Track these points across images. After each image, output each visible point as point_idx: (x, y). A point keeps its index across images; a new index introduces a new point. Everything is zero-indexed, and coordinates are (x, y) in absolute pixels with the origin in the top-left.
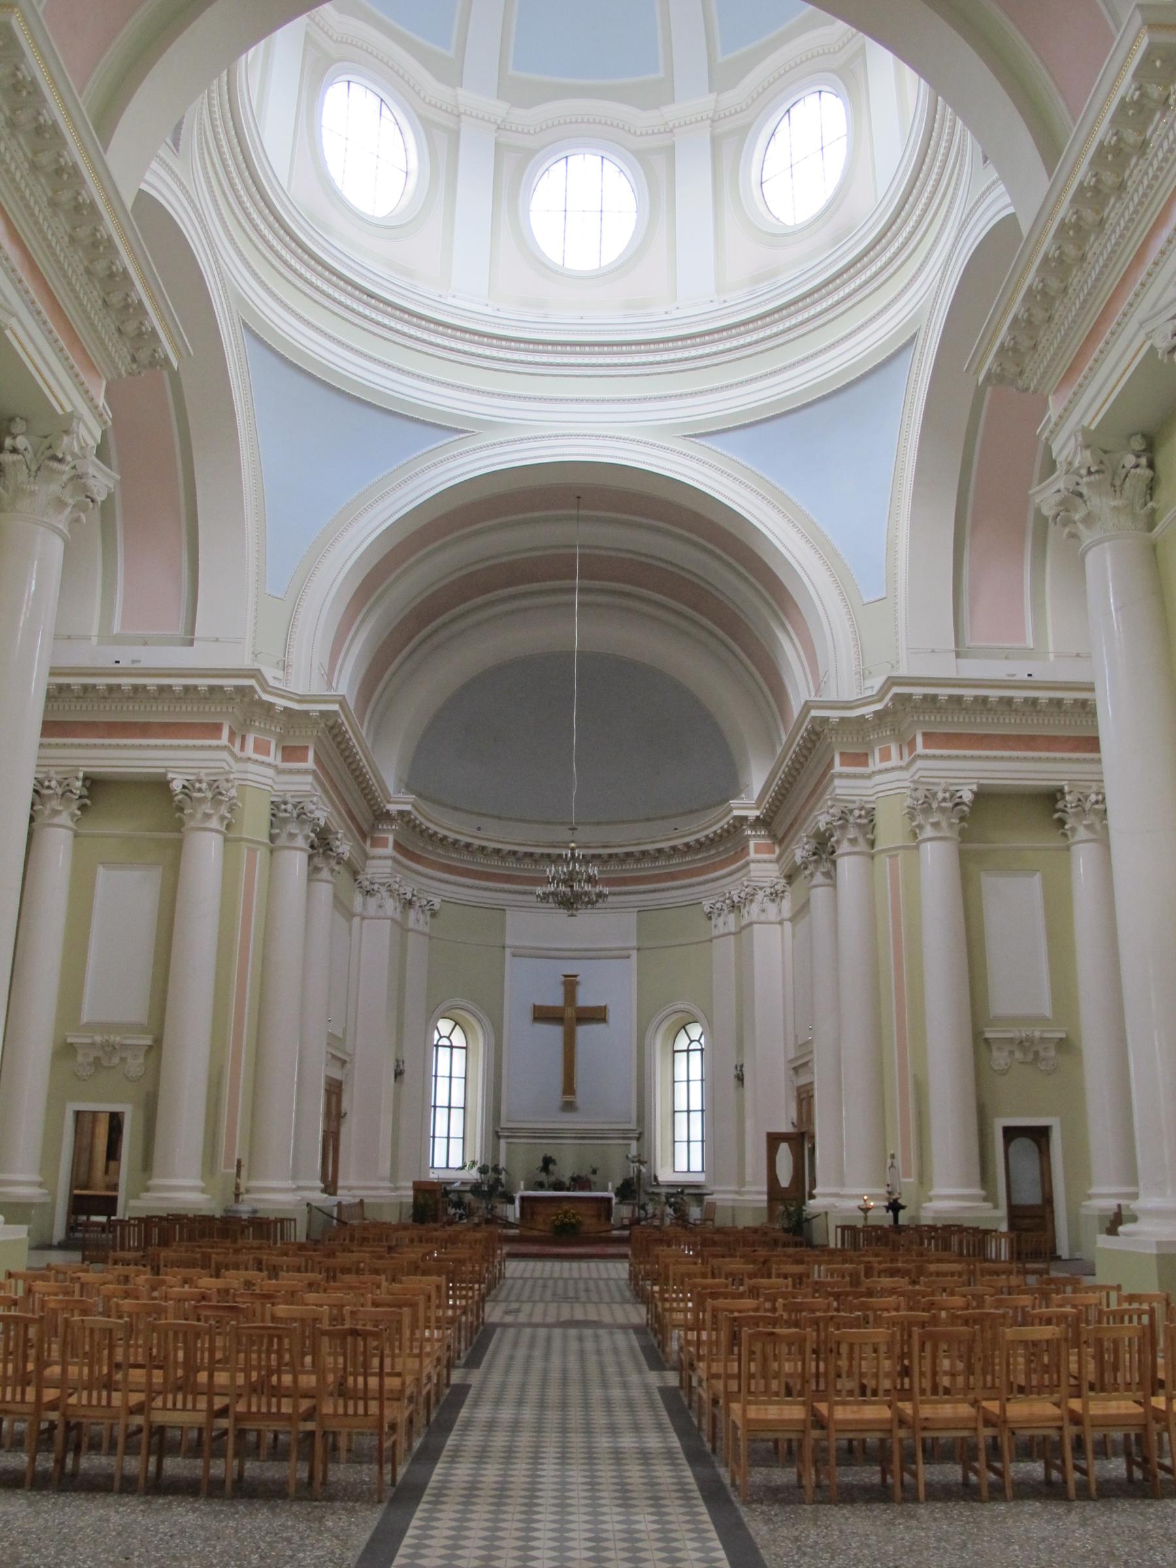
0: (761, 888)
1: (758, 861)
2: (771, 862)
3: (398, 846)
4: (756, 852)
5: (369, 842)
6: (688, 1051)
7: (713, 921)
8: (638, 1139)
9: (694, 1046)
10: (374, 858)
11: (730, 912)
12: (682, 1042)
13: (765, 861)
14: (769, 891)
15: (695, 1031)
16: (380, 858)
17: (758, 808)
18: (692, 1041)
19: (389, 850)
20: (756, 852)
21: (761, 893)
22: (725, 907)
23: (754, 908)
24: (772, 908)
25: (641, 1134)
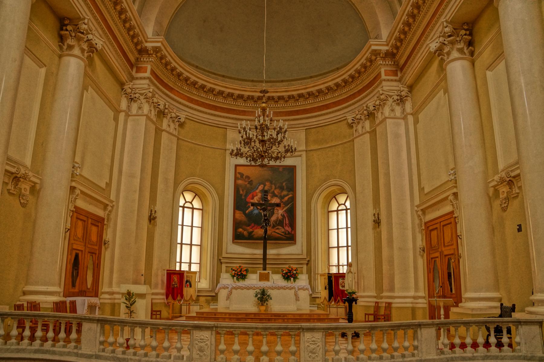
0: (391, 96)
1: (388, 80)
2: (396, 81)
3: (153, 73)
4: (385, 75)
5: (135, 70)
6: (337, 211)
7: (354, 128)
8: (307, 264)
9: (343, 207)
10: (137, 78)
11: (366, 119)
12: (334, 206)
13: (392, 80)
14: (396, 98)
15: (342, 199)
16: (141, 78)
17: (387, 45)
18: (339, 205)
19: (148, 74)
20: (385, 75)
21: (391, 100)
22: (363, 117)
23: (387, 111)
24: (398, 110)
25: (308, 261)
